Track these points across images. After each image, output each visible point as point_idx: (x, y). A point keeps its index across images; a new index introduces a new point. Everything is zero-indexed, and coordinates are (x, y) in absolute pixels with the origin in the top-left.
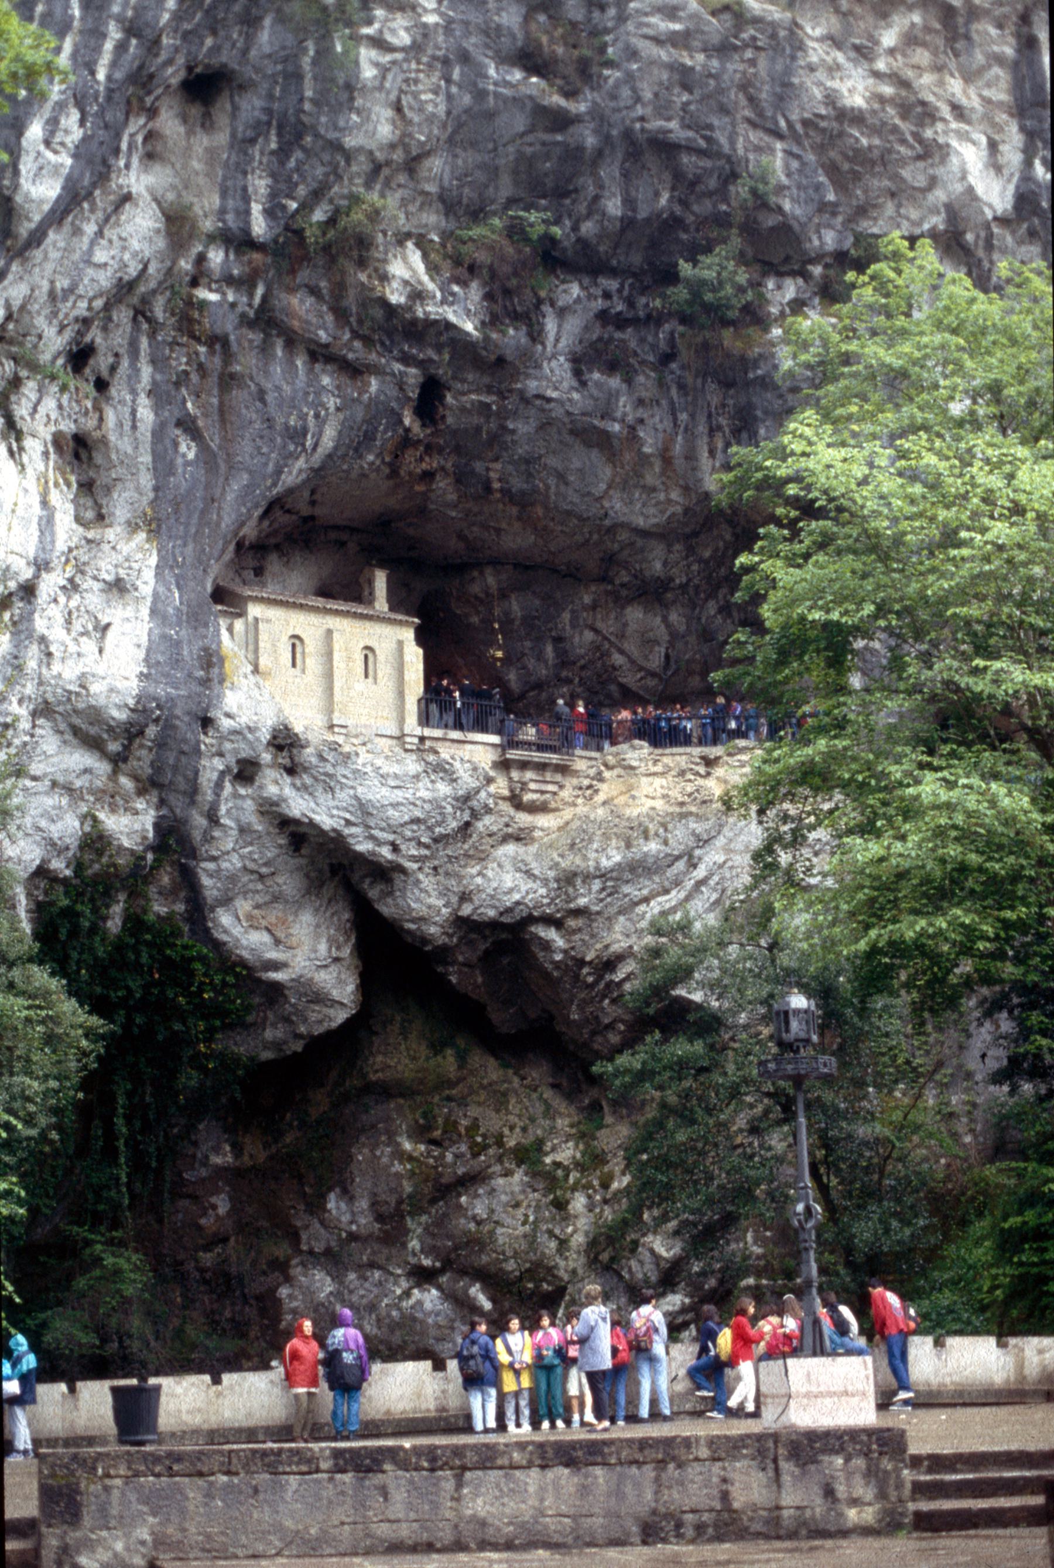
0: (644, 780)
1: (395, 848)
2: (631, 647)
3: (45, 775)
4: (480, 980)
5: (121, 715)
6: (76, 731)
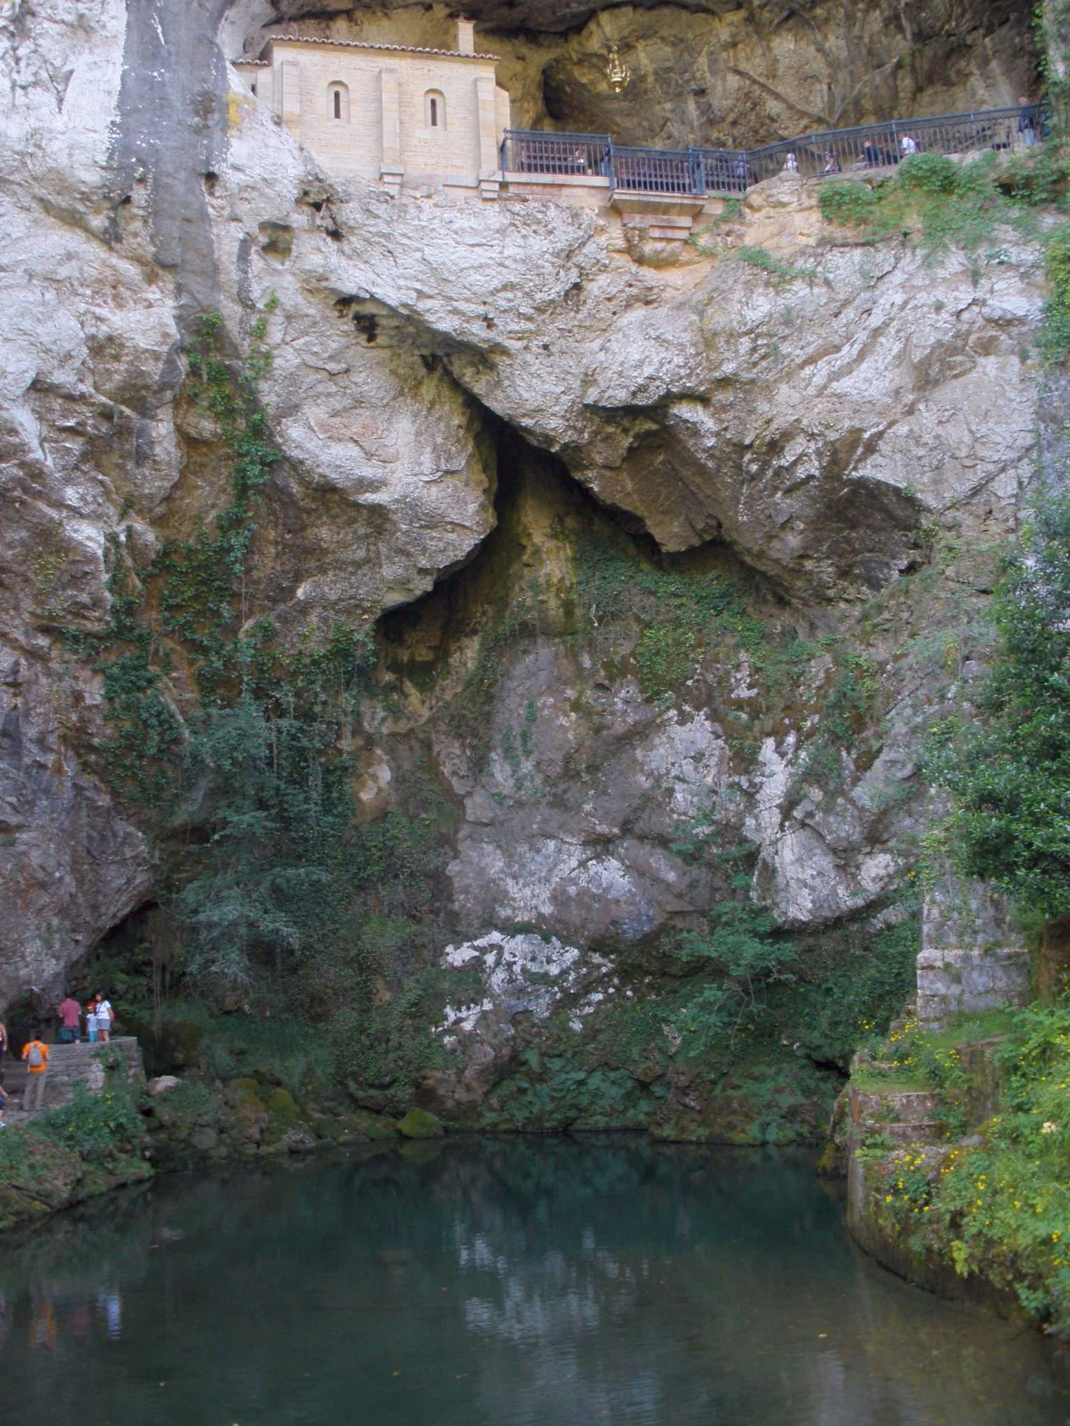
1: (489, 323)
4: (630, 486)
5: (93, 177)
6: (46, 206)
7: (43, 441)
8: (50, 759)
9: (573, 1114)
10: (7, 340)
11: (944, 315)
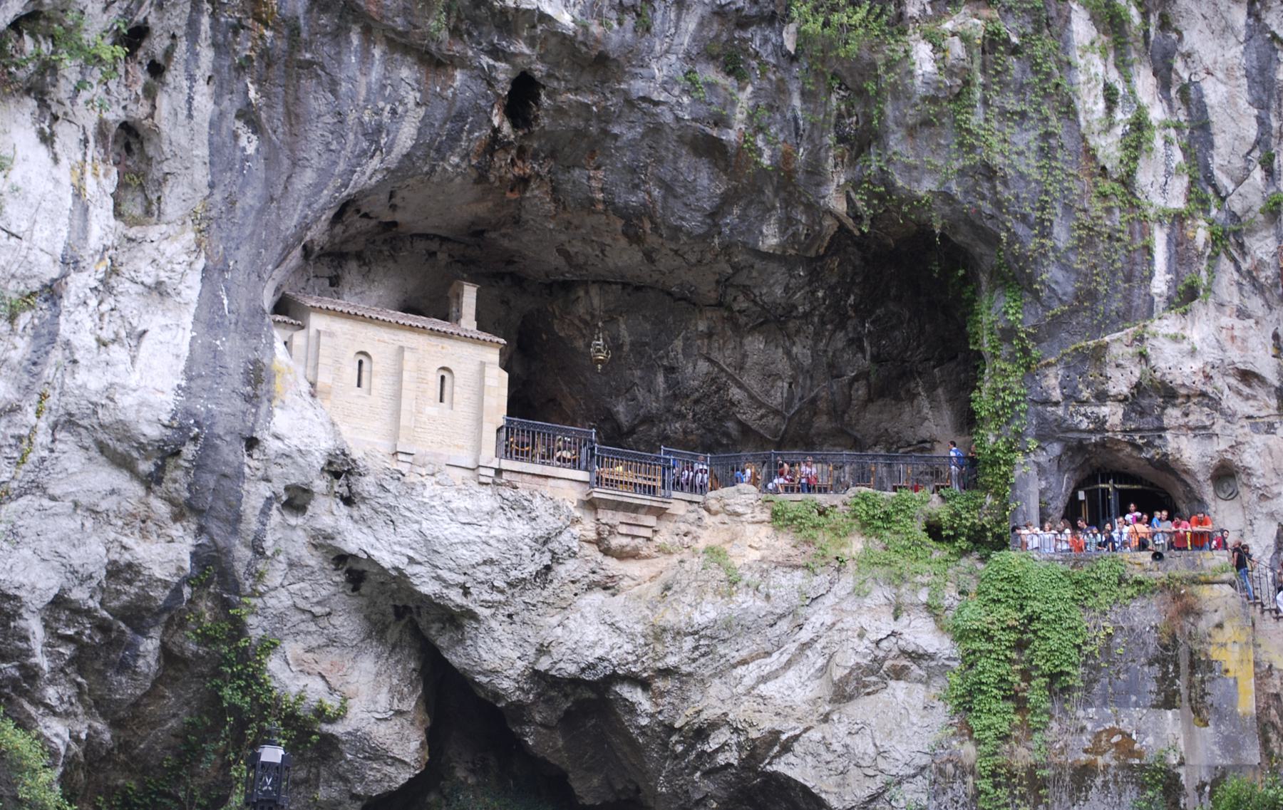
0: (750, 528)
1: (466, 592)
2: (752, 381)
3: (67, 494)
4: (560, 743)
5: (153, 432)
6: (102, 448)
7: (44, 645)
10: (43, 560)
11: (866, 642)
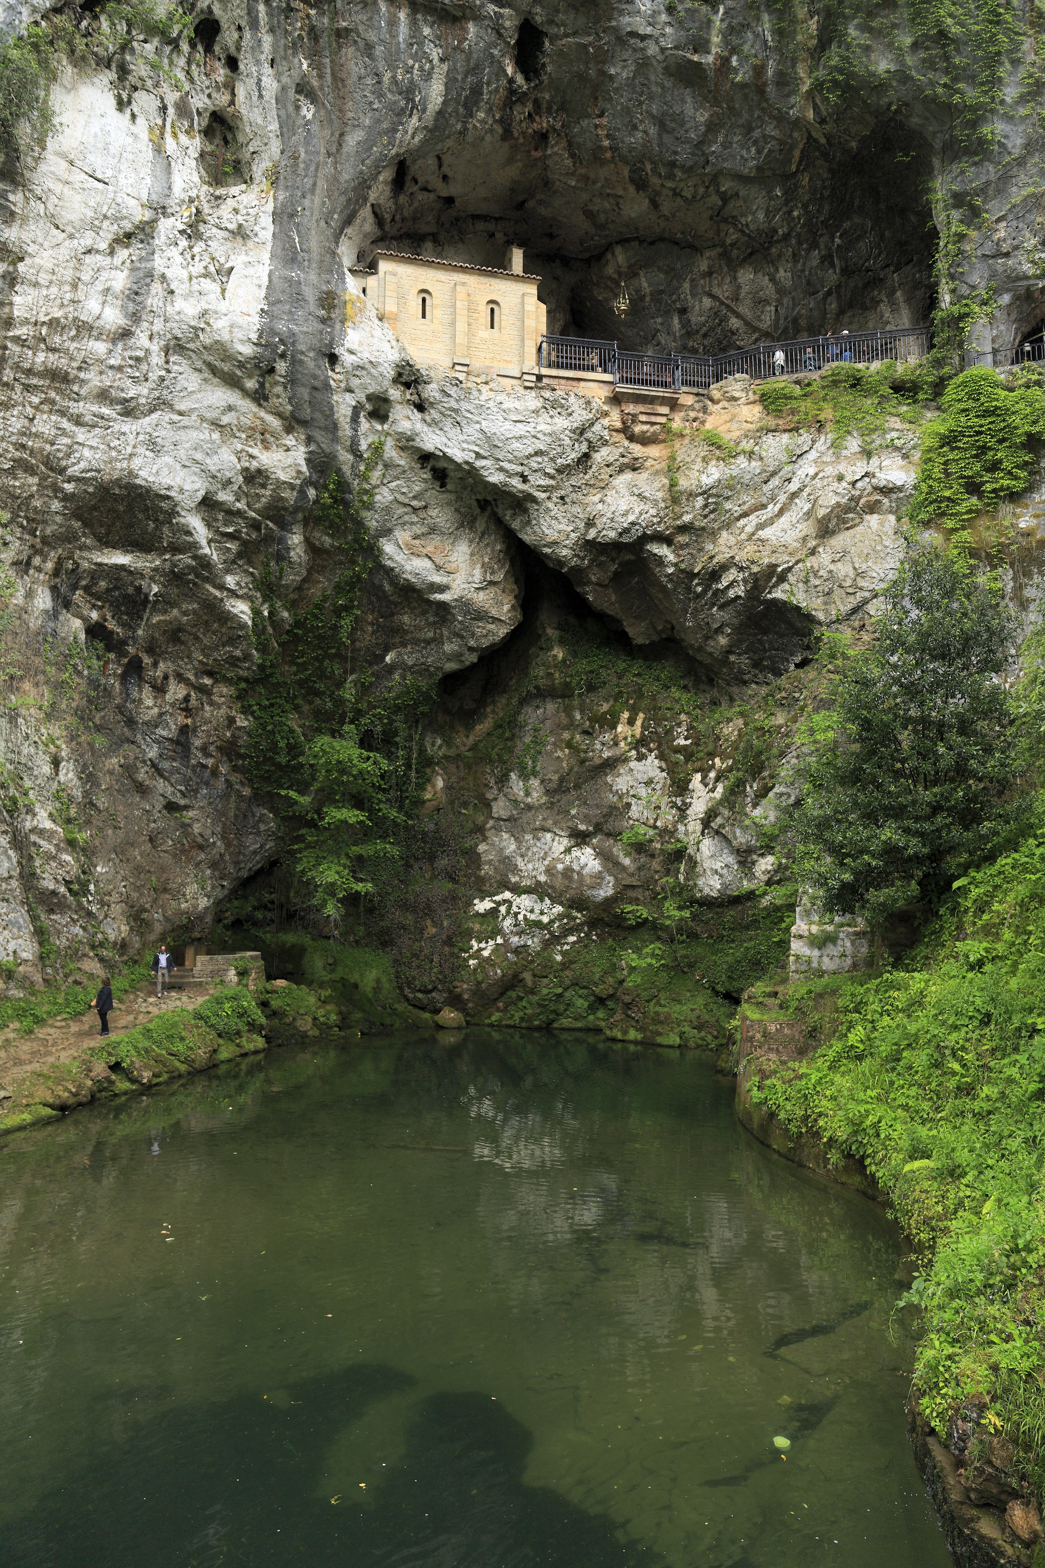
1: (525, 479)
4: (613, 598)
5: (247, 350)
7: (210, 542)
8: (210, 762)
9: (552, 1017)
10: (184, 466)
11: (844, 484)
